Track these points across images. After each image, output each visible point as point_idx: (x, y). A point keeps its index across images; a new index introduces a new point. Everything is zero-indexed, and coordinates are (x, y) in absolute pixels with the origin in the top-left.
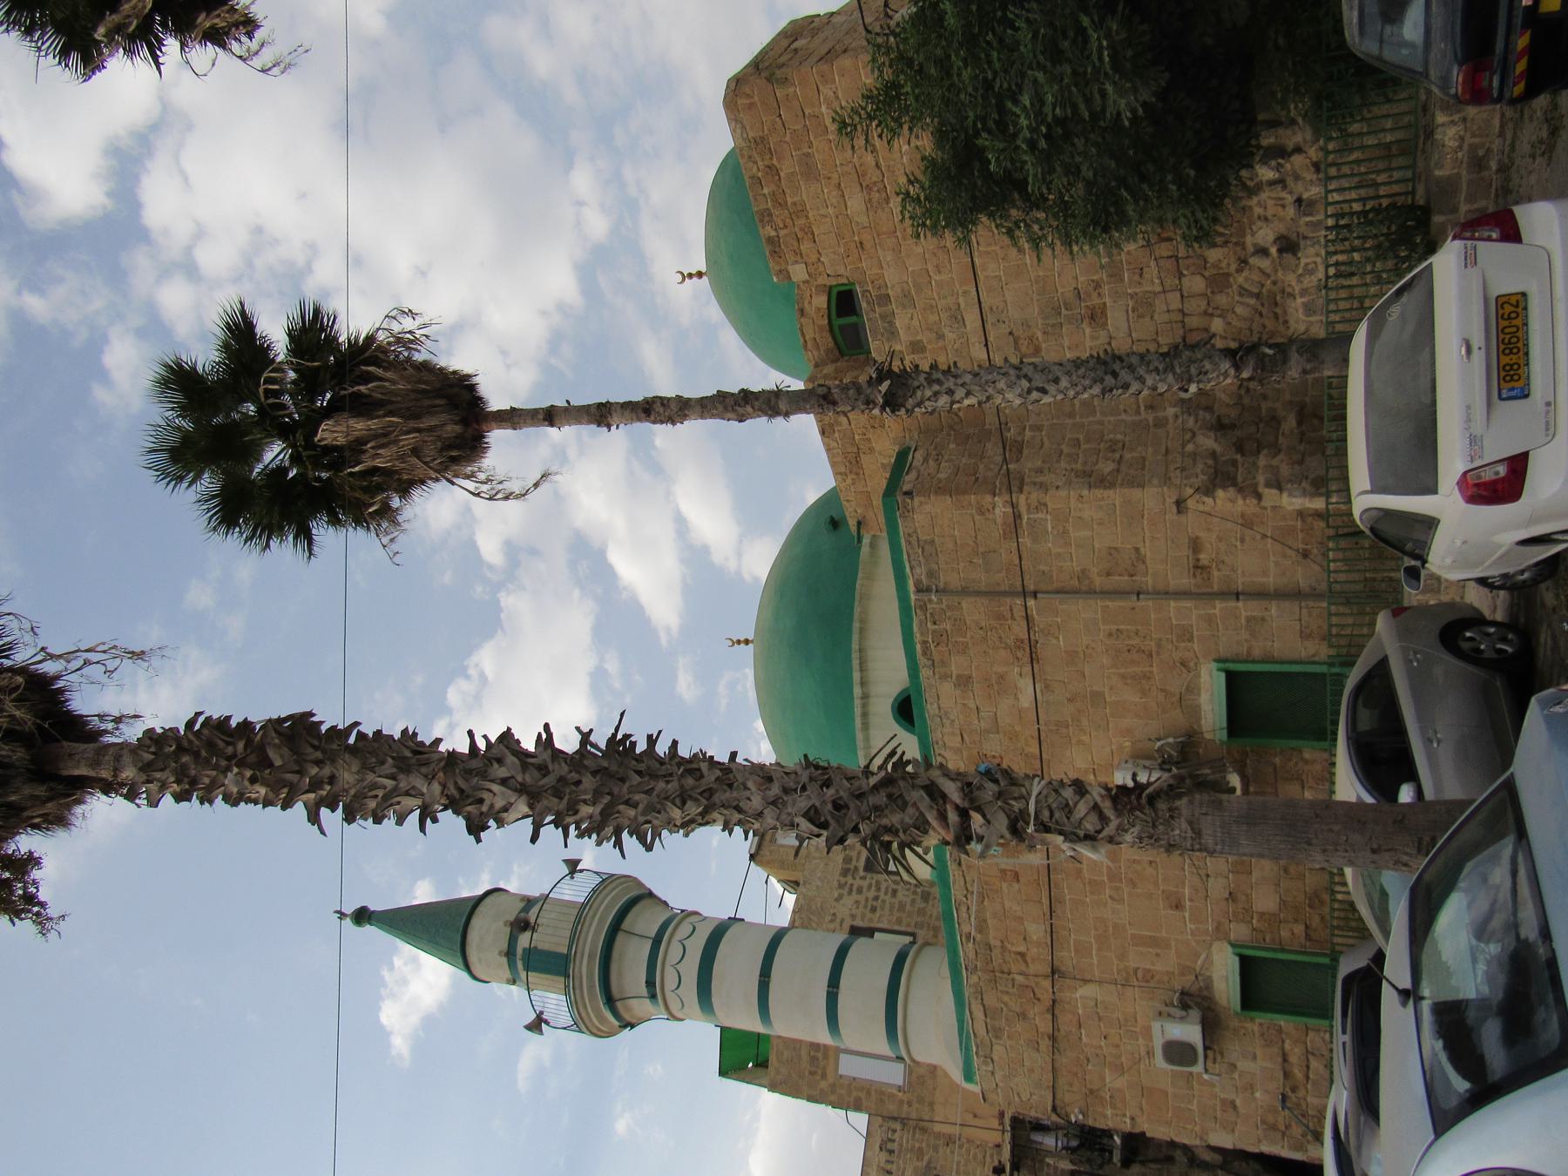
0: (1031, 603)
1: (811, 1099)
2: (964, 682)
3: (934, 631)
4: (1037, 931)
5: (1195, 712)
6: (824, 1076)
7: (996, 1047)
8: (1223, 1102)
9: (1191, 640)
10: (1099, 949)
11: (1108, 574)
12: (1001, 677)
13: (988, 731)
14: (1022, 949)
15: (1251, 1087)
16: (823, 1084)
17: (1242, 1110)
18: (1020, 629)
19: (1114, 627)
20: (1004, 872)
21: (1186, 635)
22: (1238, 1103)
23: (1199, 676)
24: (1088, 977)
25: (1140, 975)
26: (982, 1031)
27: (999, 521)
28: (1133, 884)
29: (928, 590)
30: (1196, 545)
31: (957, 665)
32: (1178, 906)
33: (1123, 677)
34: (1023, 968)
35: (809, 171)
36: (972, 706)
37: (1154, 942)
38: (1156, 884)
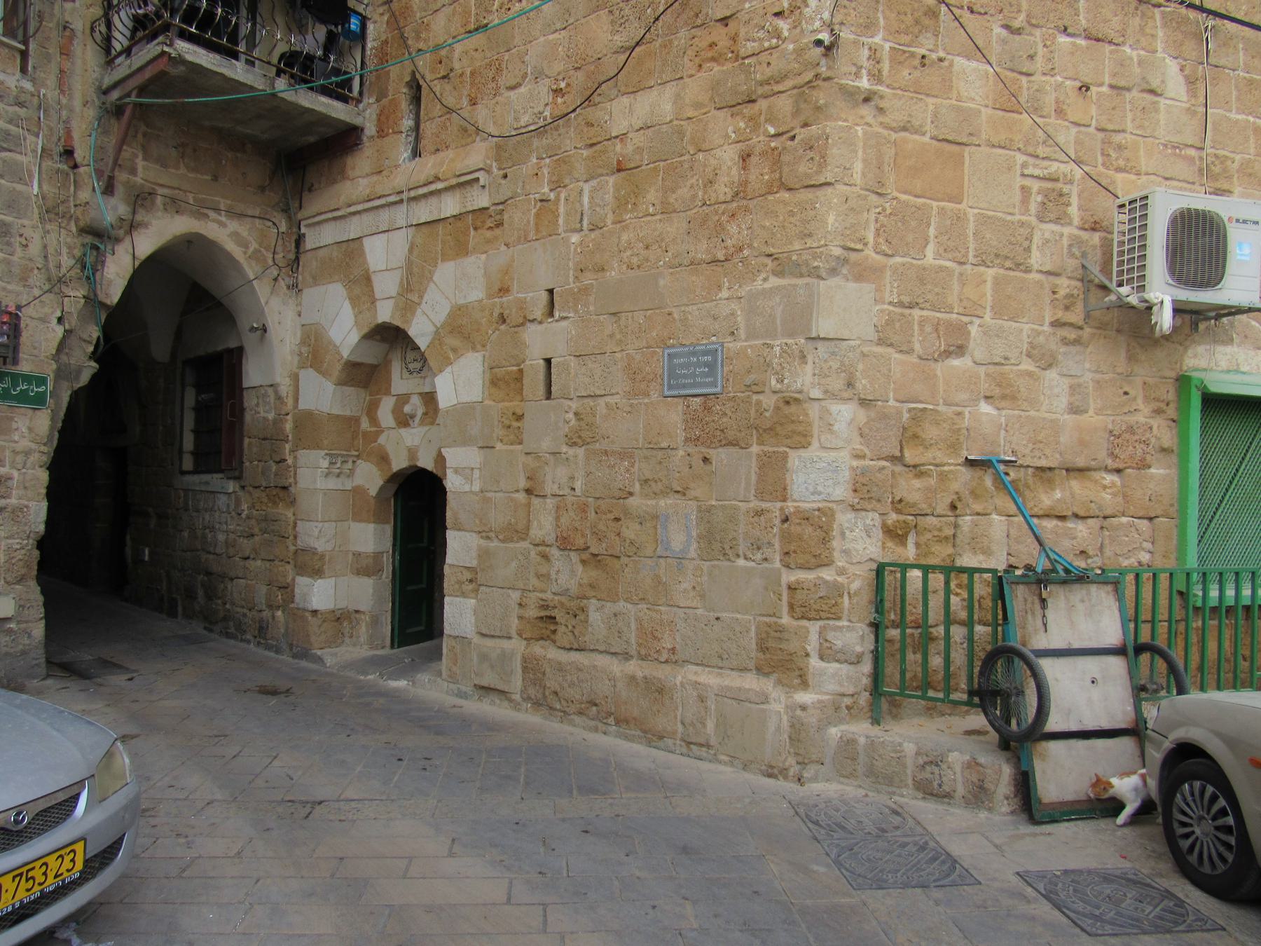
8: (962, 330)
15: (1004, 394)
22: (956, 362)
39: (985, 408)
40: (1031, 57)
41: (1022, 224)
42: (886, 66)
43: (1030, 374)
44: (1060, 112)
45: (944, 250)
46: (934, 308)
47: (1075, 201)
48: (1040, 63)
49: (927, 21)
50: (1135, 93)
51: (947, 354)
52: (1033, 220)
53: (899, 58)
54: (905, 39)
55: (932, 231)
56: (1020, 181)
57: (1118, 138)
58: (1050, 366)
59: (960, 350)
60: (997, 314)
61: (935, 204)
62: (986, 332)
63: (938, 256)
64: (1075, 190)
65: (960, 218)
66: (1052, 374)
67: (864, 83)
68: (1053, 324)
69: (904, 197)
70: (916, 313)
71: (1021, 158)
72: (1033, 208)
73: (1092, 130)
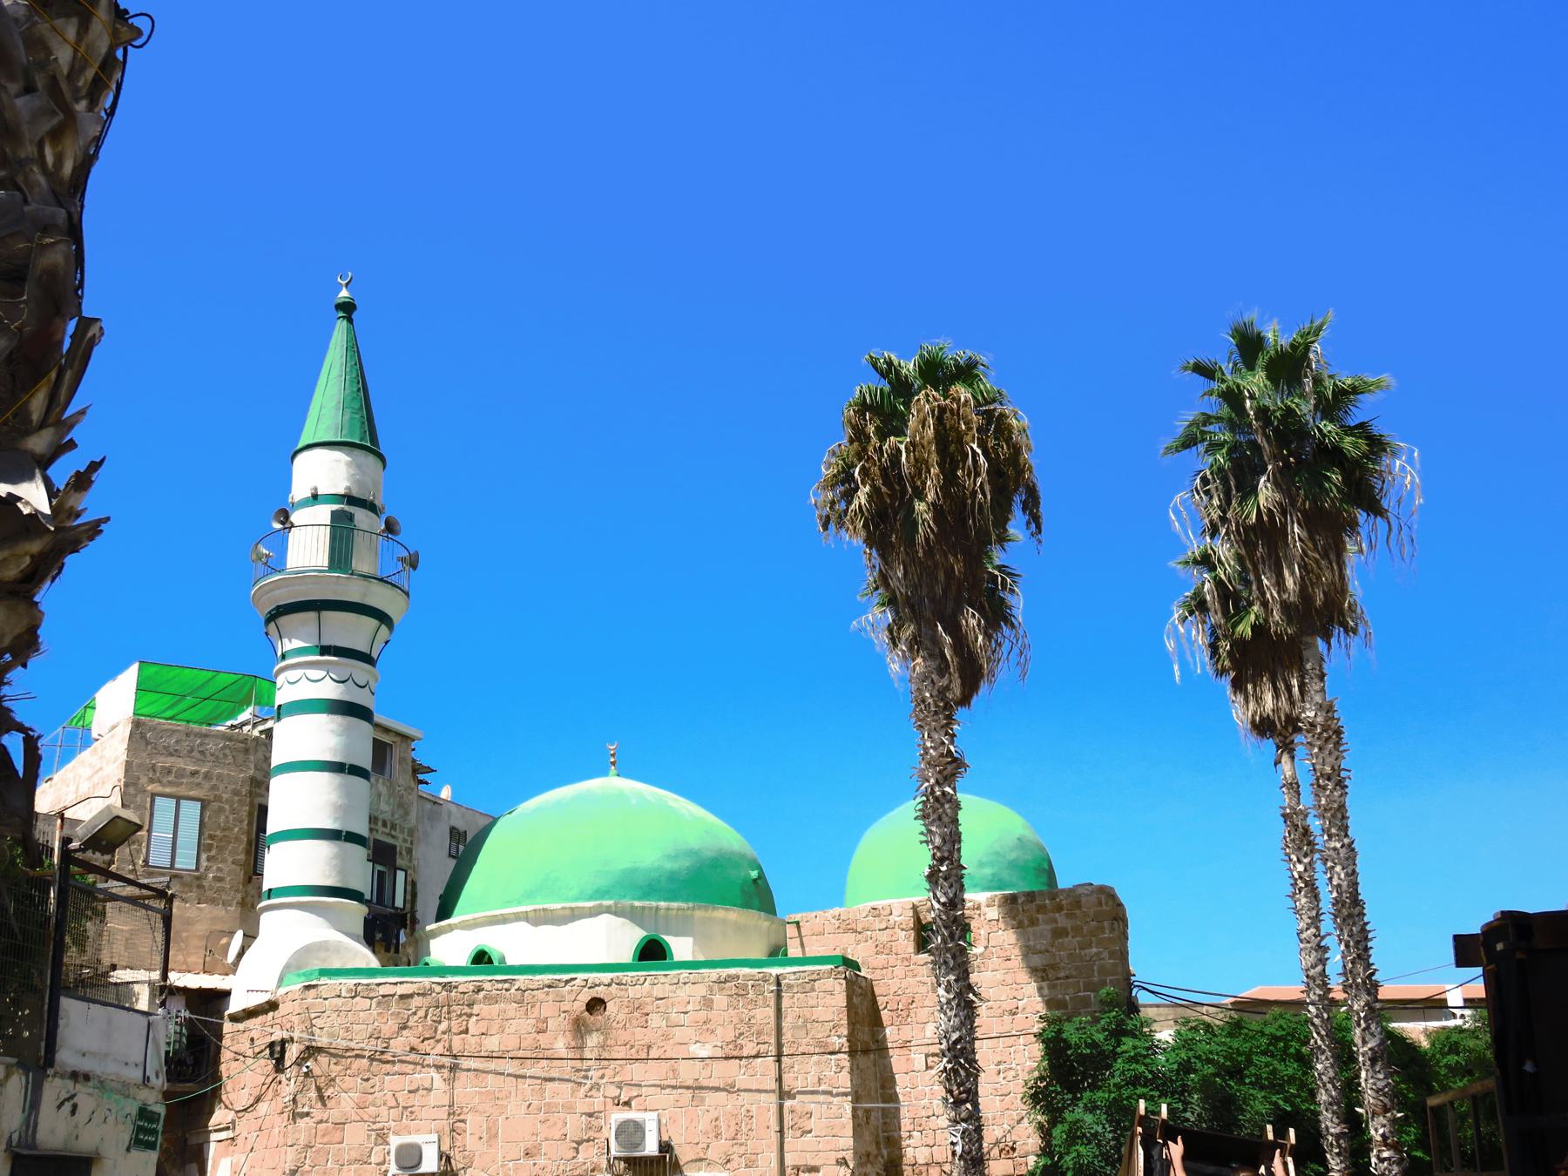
1: (128, 765)
2: (707, 1003)
4: (492, 1044)
6: (152, 781)
14: (471, 1031)
16: (144, 780)
18: (750, 1049)
20: (545, 1020)
26: (383, 990)
29: (779, 984)
31: (720, 1000)
35: (1059, 933)
36: (690, 1007)
67: (306, 1109)
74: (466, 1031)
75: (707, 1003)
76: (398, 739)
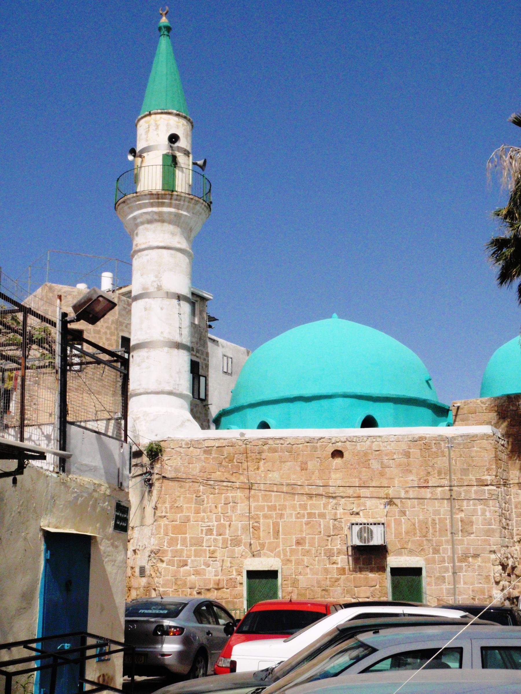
0: (448, 488)
3: (430, 443)
5: (400, 554)
7: (198, 450)
9: (434, 553)
10: (268, 506)
11: (461, 521)
12: (411, 472)
13: (382, 463)
14: (262, 469)
15: (197, 573)
17: (182, 569)
19: (437, 522)
21: (436, 551)
22: (185, 568)
23: (417, 556)
24: (251, 500)
25: (256, 524)
27: (484, 478)
28: (307, 523)
30: (476, 556)
32: (298, 543)
33: (414, 525)
34: (250, 468)
36: (395, 457)
37: (277, 533)
38: (309, 534)
39: (193, 577)
40: (203, 501)
41: (201, 537)
42: (168, 510)
43: (203, 569)
44: (211, 512)
45: (182, 545)
46: (180, 557)
47: (215, 530)
48: (205, 502)
49: (178, 499)
50: (231, 504)
51: (183, 566)
52: (204, 536)
53: (171, 508)
54: (173, 503)
55: (179, 542)
56: (200, 528)
57: (226, 515)
58: (209, 567)
59: (186, 565)
60: (195, 556)
61: (180, 536)
62: (192, 561)
63: (181, 546)
64: (215, 528)
65: (186, 538)
66: (210, 568)
67: (164, 514)
68: (210, 557)
69: (172, 535)
70: (176, 558)
71: (200, 523)
72: (204, 533)
73: (220, 514)
74: (258, 469)
75: (407, 455)
76: (198, 299)
